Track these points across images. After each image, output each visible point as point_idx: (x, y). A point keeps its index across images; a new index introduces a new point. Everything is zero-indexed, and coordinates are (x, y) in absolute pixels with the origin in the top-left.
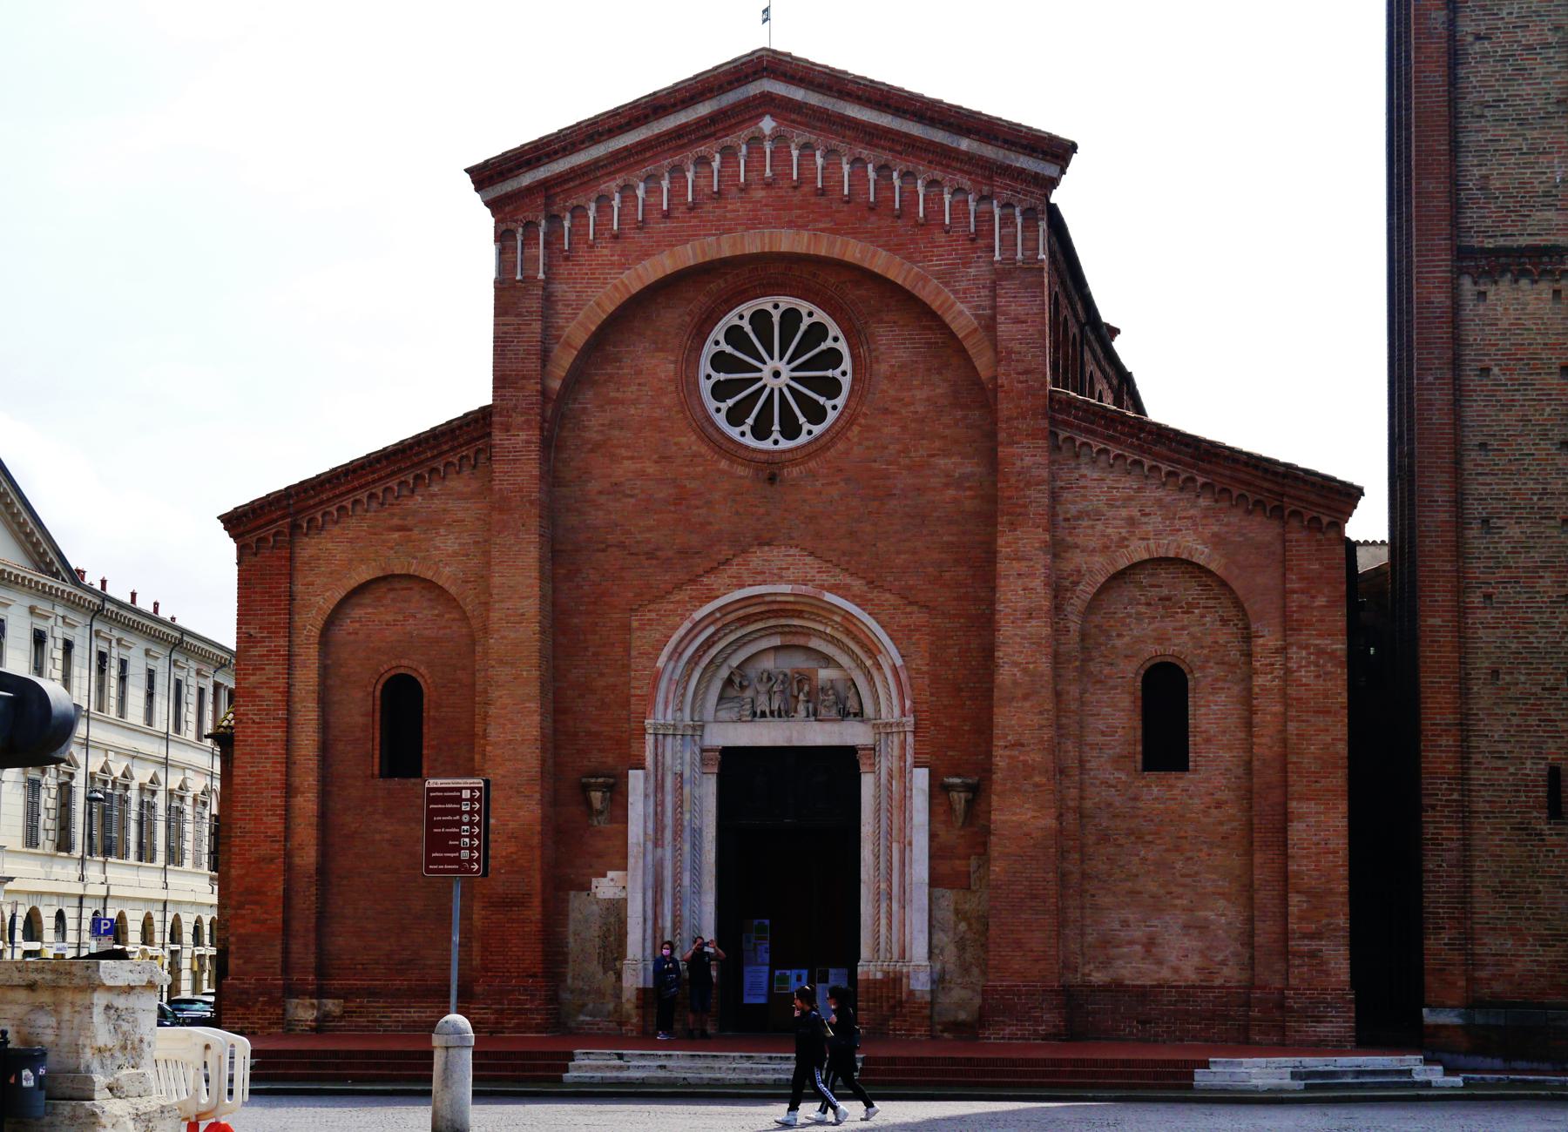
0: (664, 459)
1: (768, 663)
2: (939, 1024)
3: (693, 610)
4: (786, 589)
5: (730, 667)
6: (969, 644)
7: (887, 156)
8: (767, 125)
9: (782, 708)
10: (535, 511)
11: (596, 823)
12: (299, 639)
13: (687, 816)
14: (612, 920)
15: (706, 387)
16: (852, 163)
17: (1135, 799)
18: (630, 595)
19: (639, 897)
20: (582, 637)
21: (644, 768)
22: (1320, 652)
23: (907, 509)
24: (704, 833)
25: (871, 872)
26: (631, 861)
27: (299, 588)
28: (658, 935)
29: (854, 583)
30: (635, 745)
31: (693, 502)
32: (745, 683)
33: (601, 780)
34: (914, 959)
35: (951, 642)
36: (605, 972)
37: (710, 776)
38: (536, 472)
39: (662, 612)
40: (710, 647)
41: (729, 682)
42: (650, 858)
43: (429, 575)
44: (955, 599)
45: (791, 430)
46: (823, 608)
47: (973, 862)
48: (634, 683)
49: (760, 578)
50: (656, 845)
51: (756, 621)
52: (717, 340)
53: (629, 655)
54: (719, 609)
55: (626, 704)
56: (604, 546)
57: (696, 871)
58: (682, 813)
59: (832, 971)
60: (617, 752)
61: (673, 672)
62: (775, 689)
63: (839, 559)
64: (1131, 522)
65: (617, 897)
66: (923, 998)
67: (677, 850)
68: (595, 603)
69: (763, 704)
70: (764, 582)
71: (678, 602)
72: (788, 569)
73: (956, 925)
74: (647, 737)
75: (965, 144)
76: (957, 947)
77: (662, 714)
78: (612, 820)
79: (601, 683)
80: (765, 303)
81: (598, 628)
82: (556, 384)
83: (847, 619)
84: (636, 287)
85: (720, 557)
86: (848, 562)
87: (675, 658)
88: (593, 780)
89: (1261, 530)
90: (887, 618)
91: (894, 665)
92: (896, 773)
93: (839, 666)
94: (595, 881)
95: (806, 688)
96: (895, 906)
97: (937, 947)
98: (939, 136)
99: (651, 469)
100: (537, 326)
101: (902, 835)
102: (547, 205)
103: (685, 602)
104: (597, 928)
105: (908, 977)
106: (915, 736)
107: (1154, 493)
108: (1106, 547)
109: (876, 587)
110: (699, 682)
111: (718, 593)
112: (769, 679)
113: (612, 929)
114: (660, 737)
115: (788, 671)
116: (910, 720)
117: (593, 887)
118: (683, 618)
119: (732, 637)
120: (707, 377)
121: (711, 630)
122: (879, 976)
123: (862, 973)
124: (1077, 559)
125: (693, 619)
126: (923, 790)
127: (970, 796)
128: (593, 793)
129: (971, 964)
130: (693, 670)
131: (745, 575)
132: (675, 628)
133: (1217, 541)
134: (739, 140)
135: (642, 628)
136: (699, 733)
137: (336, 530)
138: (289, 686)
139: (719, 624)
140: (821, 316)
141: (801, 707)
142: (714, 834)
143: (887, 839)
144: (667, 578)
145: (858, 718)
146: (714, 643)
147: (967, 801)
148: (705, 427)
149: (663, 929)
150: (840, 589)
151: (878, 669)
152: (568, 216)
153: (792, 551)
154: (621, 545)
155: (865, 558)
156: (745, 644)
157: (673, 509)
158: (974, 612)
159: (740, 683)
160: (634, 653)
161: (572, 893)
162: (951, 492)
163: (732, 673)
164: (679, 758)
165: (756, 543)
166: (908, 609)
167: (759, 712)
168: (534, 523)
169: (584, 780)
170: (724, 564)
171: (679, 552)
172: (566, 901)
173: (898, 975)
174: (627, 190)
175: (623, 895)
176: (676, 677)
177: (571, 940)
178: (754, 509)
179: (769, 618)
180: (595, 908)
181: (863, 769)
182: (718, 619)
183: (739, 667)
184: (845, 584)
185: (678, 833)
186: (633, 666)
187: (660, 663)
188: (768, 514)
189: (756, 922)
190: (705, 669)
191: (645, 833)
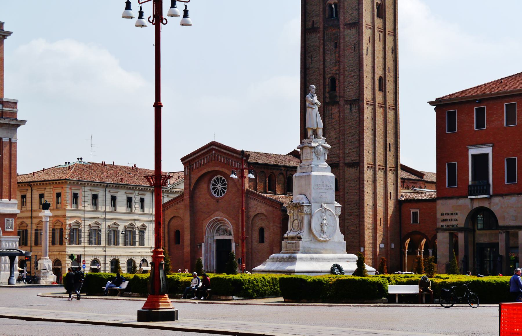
0: (205, 199)
1: (222, 227)
7: (227, 156)
8: (214, 152)
10: (189, 207)
12: (165, 225)
15: (211, 188)
16: (223, 157)
17: (258, 247)
22: (277, 226)
27: (165, 218)
30: (203, 239)
38: (189, 202)
40: (213, 226)
41: (217, 230)
43: (179, 216)
45: (221, 195)
50: (206, 254)
52: (212, 182)
57: (213, 257)
61: (208, 229)
64: (256, 208)
69: (221, 234)
70: (217, 217)
75: (235, 155)
77: (207, 235)
80: (218, 176)
82: (192, 189)
84: (200, 175)
89: (271, 209)
98: (232, 154)
99: (204, 201)
100: (189, 181)
102: (190, 164)
107: (259, 204)
108: (254, 211)
118: (208, 222)
119: (216, 224)
120: (212, 187)
124: (251, 213)
132: (207, 223)
133: (266, 211)
134: (210, 154)
137: (169, 210)
138: (164, 232)
139: (213, 222)
140: (224, 178)
146: (214, 225)
148: (211, 194)
152: (192, 165)
153: (220, 212)
162: (237, 204)
164: (210, 241)
168: (189, 209)
174: (198, 161)
183: (218, 228)
185: (210, 252)
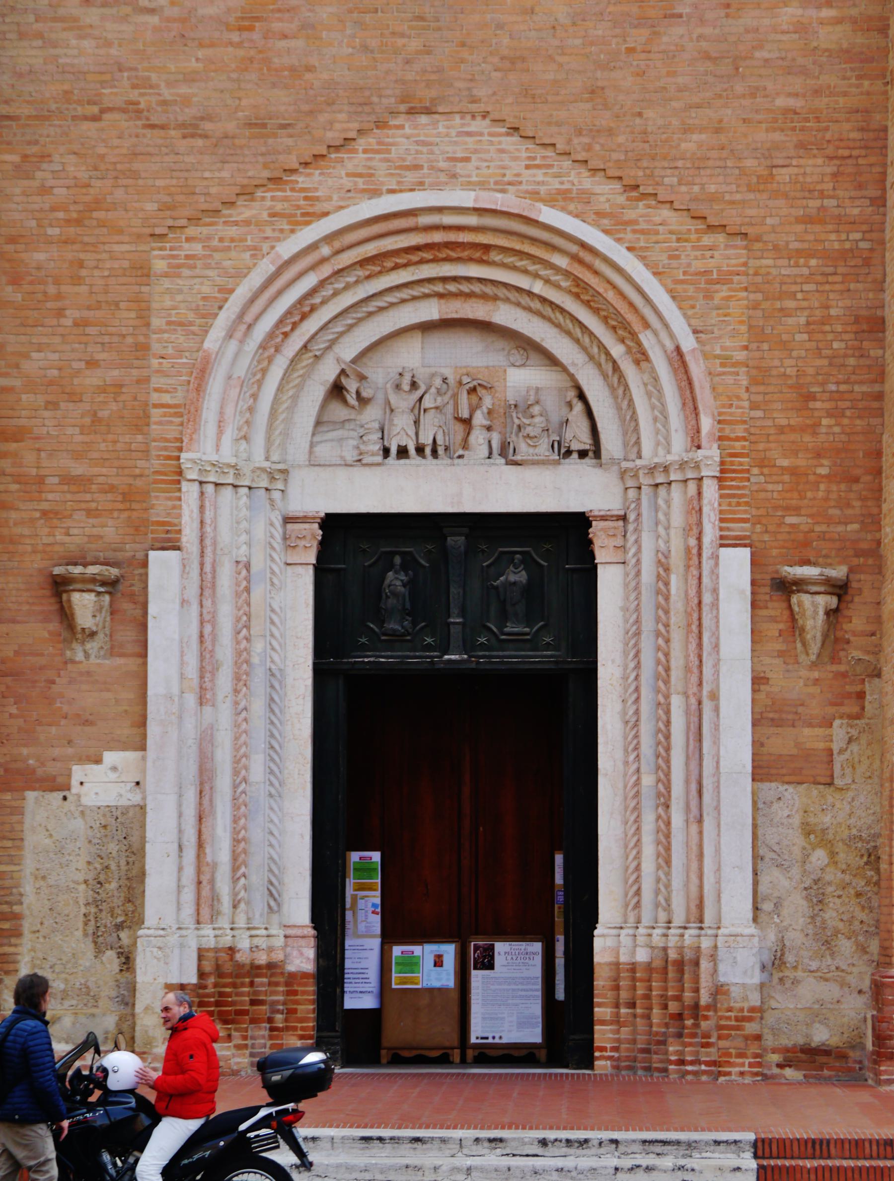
2: (774, 1051)
3: (278, 240)
4: (467, 199)
5: (338, 360)
6: (828, 307)
9: (440, 441)
11: (80, 656)
13: (258, 646)
14: (113, 847)
18: (151, 207)
19: (170, 802)
20: (52, 290)
21: (178, 548)
23: (704, 44)
24: (289, 681)
25: (619, 754)
26: (153, 730)
28: (205, 879)
29: (598, 189)
31: (277, 26)
32: (365, 394)
33: (92, 570)
34: (724, 922)
35: (790, 304)
36: (99, 951)
37: (300, 570)
39: (215, 243)
40: (304, 317)
41: (337, 390)
42: (190, 725)
44: (799, 220)
46: (534, 240)
47: (839, 731)
48: (157, 381)
49: (410, 177)
51: (396, 267)
53: (148, 325)
54: (329, 238)
55: (141, 423)
56: (95, 109)
57: (274, 750)
58: (248, 639)
59: (501, 948)
60: (125, 515)
62: (427, 402)
63: (569, 141)
65: (123, 802)
66: (745, 998)
67: (240, 711)
68: (78, 222)
70: (420, 186)
71: (247, 223)
72: (467, 160)
73: (805, 860)
74: (185, 486)
76: (808, 898)
78: (113, 651)
79: (92, 379)
81: (84, 272)
83: (581, 262)
85: (329, 135)
86: (588, 148)
87: (239, 334)
88: (77, 570)
90: (664, 259)
91: (678, 349)
92: (677, 560)
93: (552, 361)
94: (78, 772)
95: (488, 402)
96: (677, 819)
97: (766, 898)
101: (694, 679)
103: (259, 224)
104: (82, 864)
105: (713, 958)
106: (721, 488)
109: (644, 196)
110: (280, 389)
111: (326, 206)
112: (414, 385)
113: (113, 866)
114: (210, 489)
115: (448, 372)
116: (711, 454)
117: (74, 782)
118: (256, 253)
121: (310, 281)
122: (642, 956)
123: (604, 949)
125: (279, 256)
126: (743, 592)
127: (833, 601)
128: (76, 597)
129: (836, 932)
130: (270, 360)
131: (381, 170)
132: (241, 274)
135: (173, 272)
136: (280, 486)
139: (326, 270)
141: (478, 438)
142: (309, 682)
143: (658, 691)
144: (225, 174)
145: (587, 460)
146: (313, 309)
147: (829, 613)
149: (214, 866)
150: (572, 199)
151: (637, 362)
154: (132, 109)
155: (621, 139)
156: (370, 314)
157: (235, 37)
158: (836, 246)
159: (358, 393)
160: (157, 322)
161: (31, 795)
163: (343, 372)
165: (403, 108)
166: (707, 240)
167: (394, 450)
169: (57, 571)
170: (337, 148)
171: (250, 125)
172: (19, 811)
173: (689, 955)
175: (135, 798)
176: (241, 371)
177: (28, 888)
178: (400, 42)
179: (422, 262)
180: (78, 825)
181: (600, 556)
182: (323, 260)
184: (583, 192)
185: (241, 680)
186: (156, 347)
187: (212, 342)
188: (427, 51)
189: (355, 857)
190: (294, 361)
191: (182, 676)
